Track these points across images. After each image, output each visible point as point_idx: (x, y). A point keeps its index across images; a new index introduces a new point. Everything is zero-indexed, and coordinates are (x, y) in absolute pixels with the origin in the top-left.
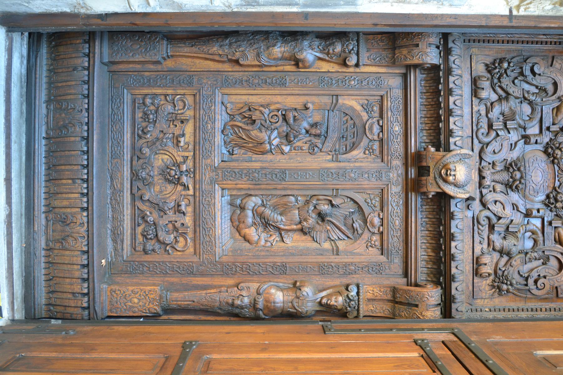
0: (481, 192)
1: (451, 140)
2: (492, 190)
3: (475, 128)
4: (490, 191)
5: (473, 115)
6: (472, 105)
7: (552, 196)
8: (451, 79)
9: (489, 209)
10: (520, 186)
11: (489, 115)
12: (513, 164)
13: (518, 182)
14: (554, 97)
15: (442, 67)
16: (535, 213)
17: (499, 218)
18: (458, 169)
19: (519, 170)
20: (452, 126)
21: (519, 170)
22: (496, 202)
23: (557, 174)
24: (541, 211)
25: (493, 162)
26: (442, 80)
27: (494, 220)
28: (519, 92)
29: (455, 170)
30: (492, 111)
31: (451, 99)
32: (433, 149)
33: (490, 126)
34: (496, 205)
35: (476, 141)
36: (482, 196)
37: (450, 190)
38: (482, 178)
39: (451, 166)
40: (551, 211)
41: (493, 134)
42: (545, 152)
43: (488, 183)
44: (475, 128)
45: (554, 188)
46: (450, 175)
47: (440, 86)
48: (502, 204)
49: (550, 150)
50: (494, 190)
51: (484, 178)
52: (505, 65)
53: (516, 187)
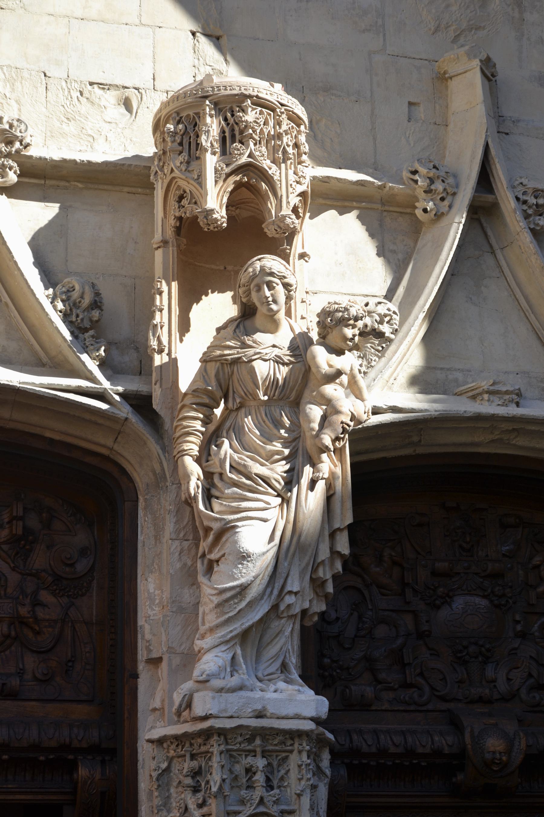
0: (497, 700)
1: (446, 752)
2: (493, 684)
3: (412, 708)
4: (495, 686)
5: (396, 709)
6: (382, 710)
7: (496, 602)
8: (365, 749)
9: (519, 689)
10: (488, 646)
11: (396, 686)
12: (459, 655)
13: (483, 649)
14: (366, 593)
15: (346, 761)
16: (519, 628)
17: (530, 675)
18: (492, 749)
19: (466, 647)
20: (428, 750)
21: (466, 647)
22: (509, 680)
23: (466, 592)
24: (518, 618)
25: (457, 682)
26: (364, 761)
27: (532, 680)
28: (363, 642)
29: (494, 753)
30: (390, 683)
31: (392, 750)
32: (460, 777)
33: (411, 686)
34: (512, 680)
35: (430, 707)
36: (504, 699)
37: (518, 758)
38: (481, 700)
39: (488, 756)
40: (514, 603)
41: (420, 680)
42: (438, 608)
43: (487, 691)
44: (412, 708)
45: (484, 597)
46: (500, 759)
47: (372, 763)
48: (510, 670)
49: (437, 602)
50: (494, 681)
51: (481, 697)
52: (327, 661)
53: (488, 650)
